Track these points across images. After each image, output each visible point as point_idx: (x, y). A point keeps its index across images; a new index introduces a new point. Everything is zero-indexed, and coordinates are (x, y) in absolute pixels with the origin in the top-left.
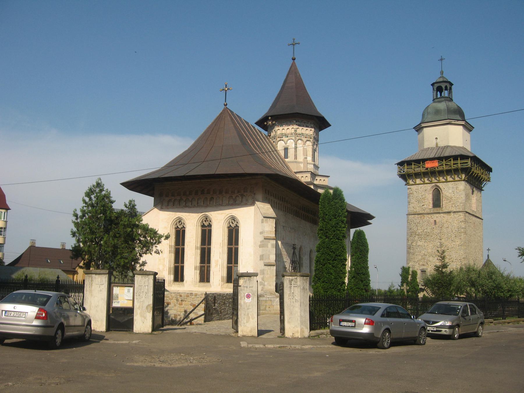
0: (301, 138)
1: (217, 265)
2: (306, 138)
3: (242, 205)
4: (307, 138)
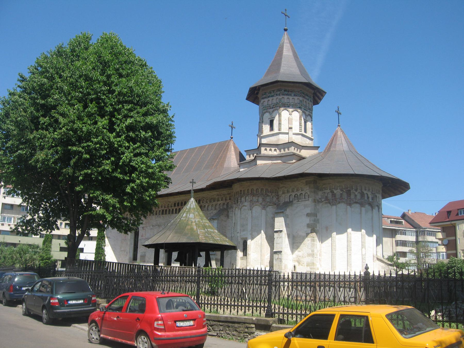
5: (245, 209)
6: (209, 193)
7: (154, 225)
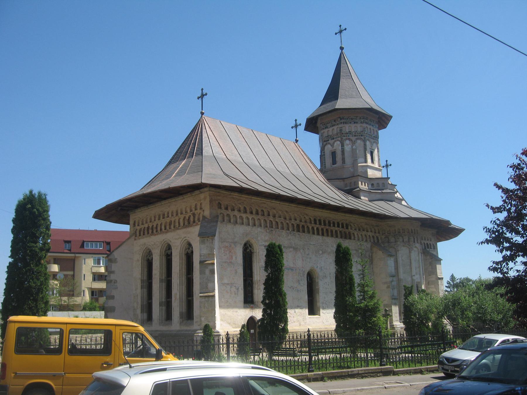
0: (349, 137)
1: (176, 299)
2: (355, 137)
3: (194, 226)
4: (357, 136)
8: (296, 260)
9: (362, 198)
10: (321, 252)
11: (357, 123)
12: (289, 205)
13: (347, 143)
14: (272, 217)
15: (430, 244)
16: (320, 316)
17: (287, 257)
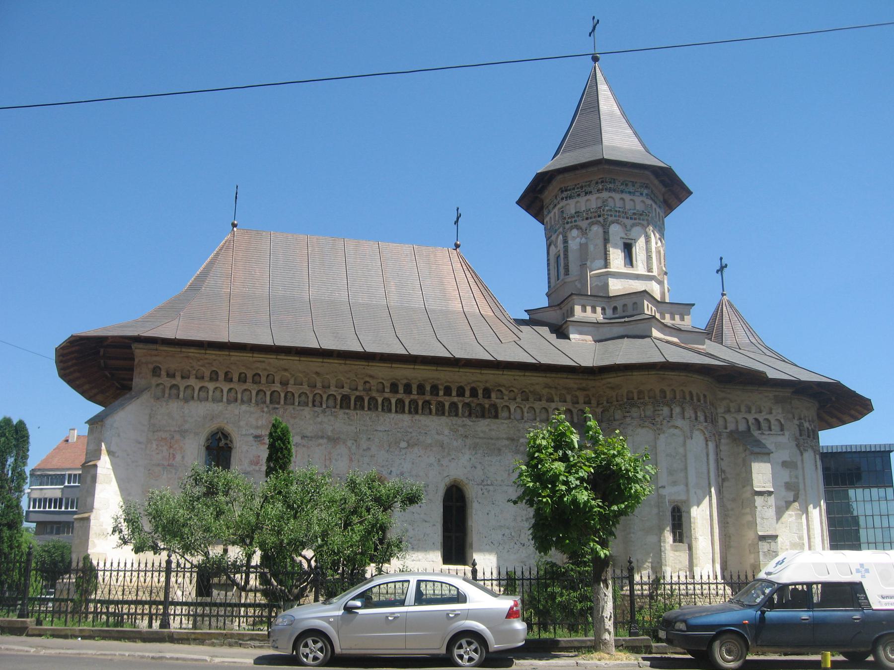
0: (576, 224)
4: (591, 218)
5: (674, 434)
6: (520, 376)
7: (309, 435)
8: (334, 461)
9: (571, 336)
10: (403, 444)
11: (591, 192)
12: (322, 362)
13: (573, 235)
14: (279, 385)
15: (767, 420)
16: (390, 564)
17: (309, 456)
